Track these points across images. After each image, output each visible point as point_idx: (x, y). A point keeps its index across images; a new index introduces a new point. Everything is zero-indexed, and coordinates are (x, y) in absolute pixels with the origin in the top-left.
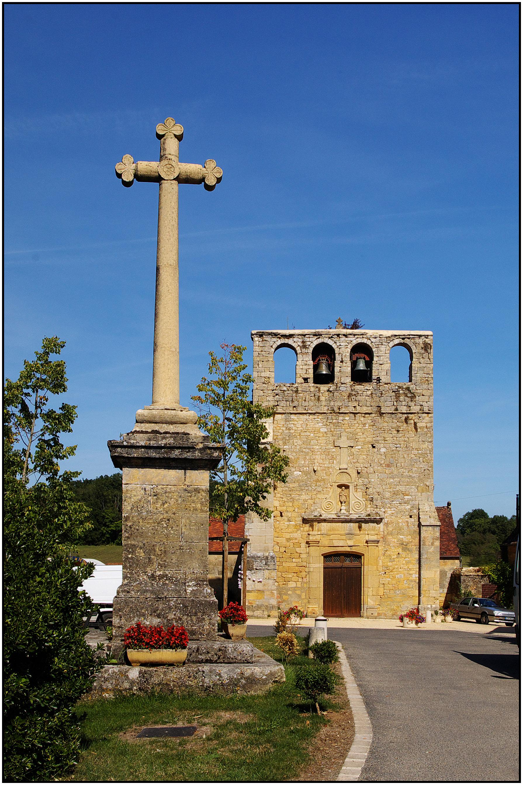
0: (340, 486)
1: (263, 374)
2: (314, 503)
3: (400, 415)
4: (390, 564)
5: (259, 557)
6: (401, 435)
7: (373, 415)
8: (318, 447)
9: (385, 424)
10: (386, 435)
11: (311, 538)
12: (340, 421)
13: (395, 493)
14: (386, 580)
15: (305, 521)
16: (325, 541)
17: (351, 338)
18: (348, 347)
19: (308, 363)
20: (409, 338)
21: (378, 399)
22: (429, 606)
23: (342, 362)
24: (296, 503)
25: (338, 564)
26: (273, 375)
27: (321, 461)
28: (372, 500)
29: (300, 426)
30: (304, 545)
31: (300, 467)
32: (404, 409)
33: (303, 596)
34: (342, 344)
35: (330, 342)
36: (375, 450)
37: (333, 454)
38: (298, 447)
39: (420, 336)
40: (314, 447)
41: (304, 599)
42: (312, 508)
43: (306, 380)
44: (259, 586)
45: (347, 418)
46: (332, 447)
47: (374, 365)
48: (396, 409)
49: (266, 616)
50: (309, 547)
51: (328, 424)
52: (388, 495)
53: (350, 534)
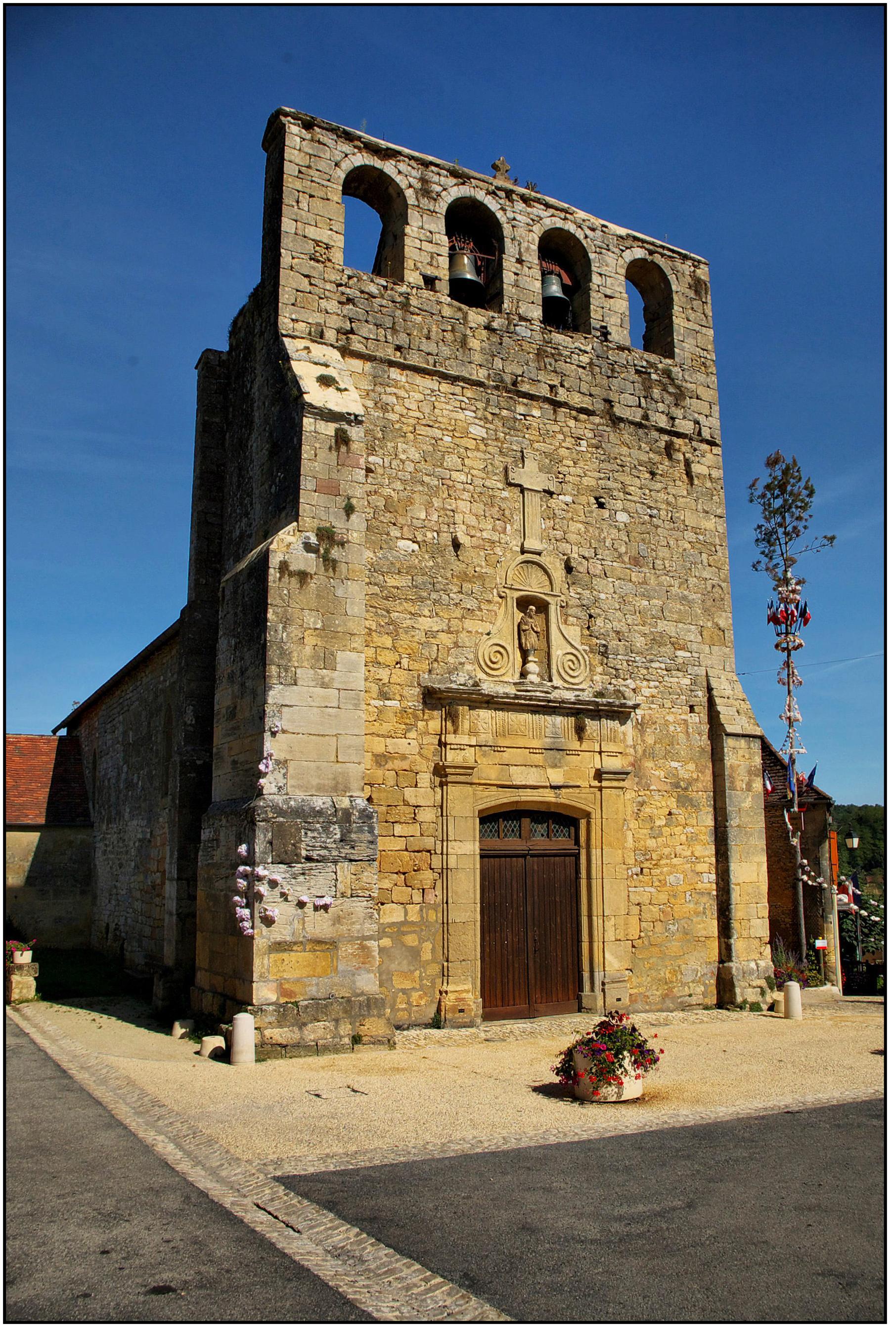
0: (523, 603)
1: (311, 232)
2: (456, 645)
3: (655, 434)
4: (651, 843)
5: (320, 813)
6: (659, 486)
7: (597, 420)
8: (463, 478)
9: (624, 450)
10: (628, 480)
11: (452, 757)
12: (519, 417)
13: (657, 640)
14: (644, 893)
15: (432, 698)
16: (488, 770)
17: (538, 210)
18: (534, 228)
19: (436, 238)
20: (662, 255)
21: (605, 382)
22: (753, 965)
23: (520, 261)
24: (404, 641)
25: (513, 843)
26: (339, 241)
27: (472, 521)
28: (604, 652)
29: (414, 406)
30: (425, 778)
31: (417, 528)
32: (662, 422)
33: (427, 955)
34: (519, 217)
35: (492, 204)
36: (606, 513)
37: (504, 506)
38: (410, 467)
39: (685, 257)
40: (455, 475)
41: (428, 962)
42: (451, 660)
43: (430, 282)
44: (319, 926)
45: (536, 413)
46: (500, 486)
47: (593, 294)
48: (646, 417)
49: (346, 1040)
50: (441, 785)
51: (490, 417)
52: (640, 642)
53: (556, 751)
